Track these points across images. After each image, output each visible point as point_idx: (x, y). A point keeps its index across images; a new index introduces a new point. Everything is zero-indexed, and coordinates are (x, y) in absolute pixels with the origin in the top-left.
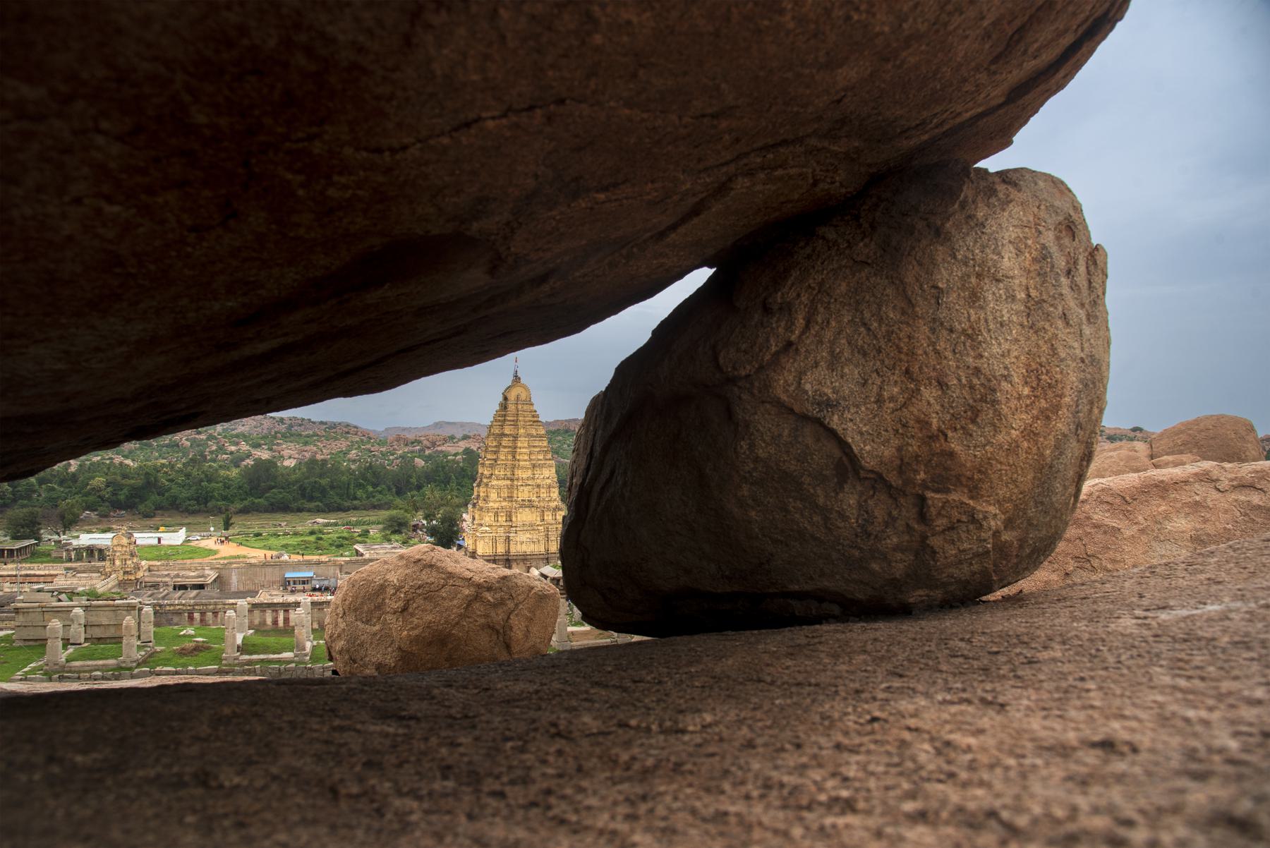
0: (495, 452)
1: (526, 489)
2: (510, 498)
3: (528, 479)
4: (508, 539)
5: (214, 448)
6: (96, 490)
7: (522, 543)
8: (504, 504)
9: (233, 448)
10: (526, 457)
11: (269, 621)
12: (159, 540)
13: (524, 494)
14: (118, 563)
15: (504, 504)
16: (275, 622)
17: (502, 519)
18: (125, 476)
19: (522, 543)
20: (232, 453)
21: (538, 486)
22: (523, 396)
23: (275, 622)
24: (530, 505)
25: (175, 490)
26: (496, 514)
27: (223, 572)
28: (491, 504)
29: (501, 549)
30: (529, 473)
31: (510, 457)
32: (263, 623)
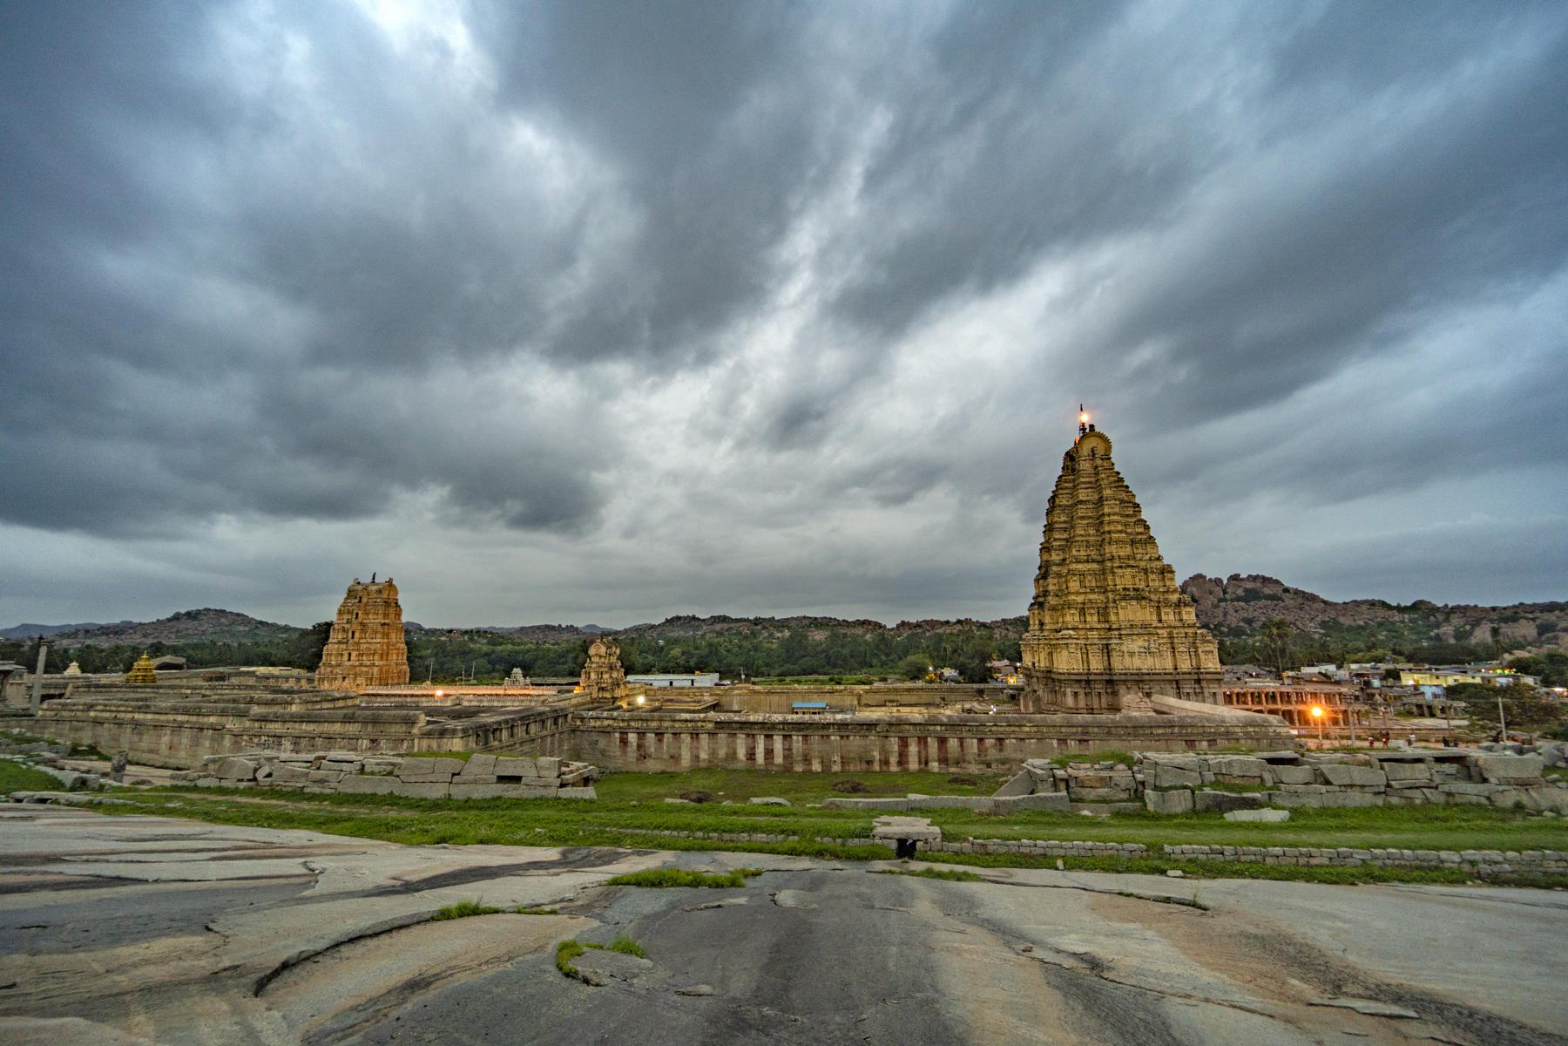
4: (1107, 650)
7: (1132, 654)
11: (741, 753)
13: (1125, 579)
16: (751, 756)
17: (1092, 620)
18: (697, 648)
21: (1146, 571)
22: (1100, 451)
23: (751, 756)
24: (1139, 596)
25: (731, 658)
26: (1082, 612)
29: (1096, 664)
31: (1092, 532)
32: (732, 756)
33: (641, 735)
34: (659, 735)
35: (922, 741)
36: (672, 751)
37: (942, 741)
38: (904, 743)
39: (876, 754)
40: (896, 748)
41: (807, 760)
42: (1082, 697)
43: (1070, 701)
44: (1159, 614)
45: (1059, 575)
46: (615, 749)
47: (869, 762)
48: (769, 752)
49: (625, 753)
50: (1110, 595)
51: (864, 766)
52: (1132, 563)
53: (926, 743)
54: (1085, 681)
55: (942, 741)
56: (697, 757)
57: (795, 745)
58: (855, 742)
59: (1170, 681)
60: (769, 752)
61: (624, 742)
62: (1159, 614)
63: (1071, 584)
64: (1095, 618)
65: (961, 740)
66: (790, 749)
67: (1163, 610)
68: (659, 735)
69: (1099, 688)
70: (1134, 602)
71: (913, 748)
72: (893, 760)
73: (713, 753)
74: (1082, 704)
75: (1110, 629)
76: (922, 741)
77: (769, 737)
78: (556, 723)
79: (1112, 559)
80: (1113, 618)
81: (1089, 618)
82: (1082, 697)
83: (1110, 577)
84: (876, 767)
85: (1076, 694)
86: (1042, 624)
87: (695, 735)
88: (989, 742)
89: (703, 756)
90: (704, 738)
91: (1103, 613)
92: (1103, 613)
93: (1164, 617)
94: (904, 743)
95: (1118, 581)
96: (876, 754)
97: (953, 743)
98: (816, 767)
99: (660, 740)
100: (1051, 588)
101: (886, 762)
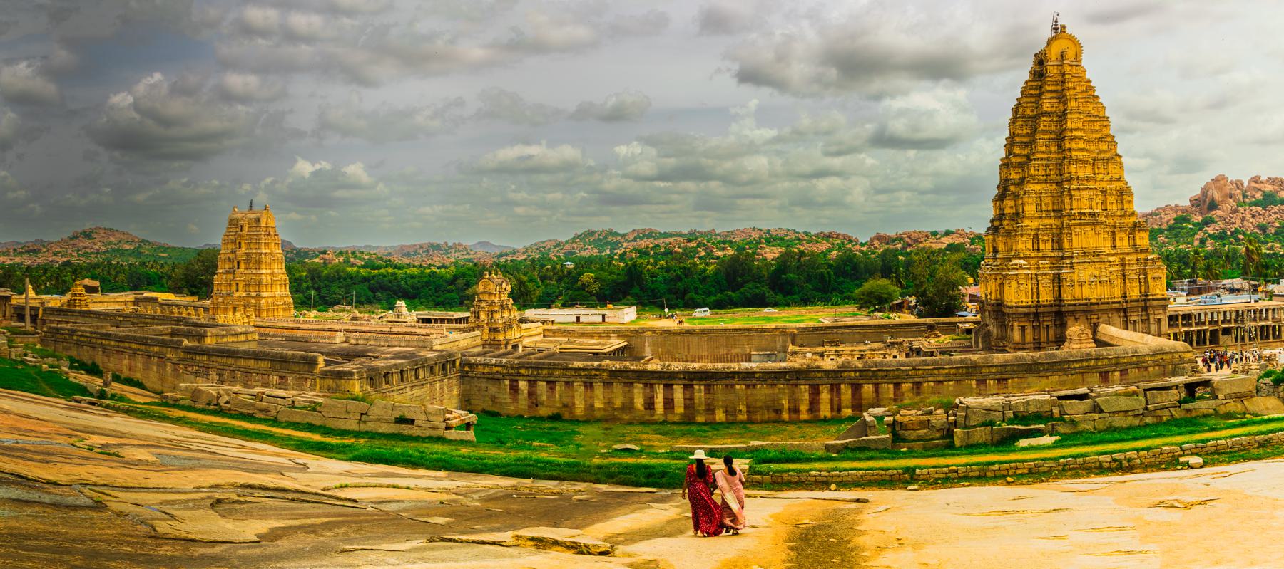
0: (1026, 145)
1: (1085, 194)
2: (1058, 213)
3: (1087, 179)
4: (1058, 280)
5: (703, 253)
6: (585, 286)
7: (1081, 284)
8: (1047, 222)
9: (720, 254)
10: (1081, 145)
11: (639, 402)
12: (603, 316)
14: (483, 316)
15: (1047, 222)
16: (650, 405)
17: (1046, 247)
19: (1081, 284)
20: (718, 258)
21: (1104, 192)
27: (636, 342)
28: (1026, 223)
30: (1088, 171)
32: (628, 406)
33: (532, 383)
34: (551, 384)
35: (835, 389)
36: (565, 400)
37: (856, 388)
38: (815, 391)
39: (785, 403)
40: (807, 396)
41: (710, 409)
42: (1029, 331)
43: (1017, 336)
44: (1114, 240)
45: (1016, 196)
46: (506, 397)
47: (778, 411)
48: (669, 403)
49: (515, 400)
50: (1066, 221)
51: (773, 415)
52: (1091, 185)
53: (839, 389)
54: (1034, 314)
55: (856, 388)
56: (592, 405)
57: (697, 395)
58: (763, 391)
59: (1118, 310)
60: (669, 403)
61: (514, 389)
62: (1114, 240)
63: (1026, 208)
64: (1049, 246)
65: (876, 386)
66: (692, 399)
67: (1118, 236)
68: (551, 384)
69: (1047, 321)
70: (1088, 228)
71: (825, 396)
72: (804, 407)
73: (609, 403)
74: (1029, 338)
75: (1063, 258)
76: (835, 389)
77: (668, 387)
78: (444, 368)
79: (1070, 180)
80: (1066, 245)
81: (1042, 246)
82: (1029, 331)
83: (1067, 200)
84: (786, 416)
85: (1023, 329)
86: (996, 251)
87: (589, 386)
88: (906, 386)
89: (598, 405)
90: (599, 390)
91: (1057, 243)
92: (1057, 243)
93: (1118, 243)
94: (815, 391)
95: (1075, 204)
96: (785, 403)
97: (868, 389)
98: (720, 416)
99: (552, 389)
100: (1007, 211)
101: (796, 410)
